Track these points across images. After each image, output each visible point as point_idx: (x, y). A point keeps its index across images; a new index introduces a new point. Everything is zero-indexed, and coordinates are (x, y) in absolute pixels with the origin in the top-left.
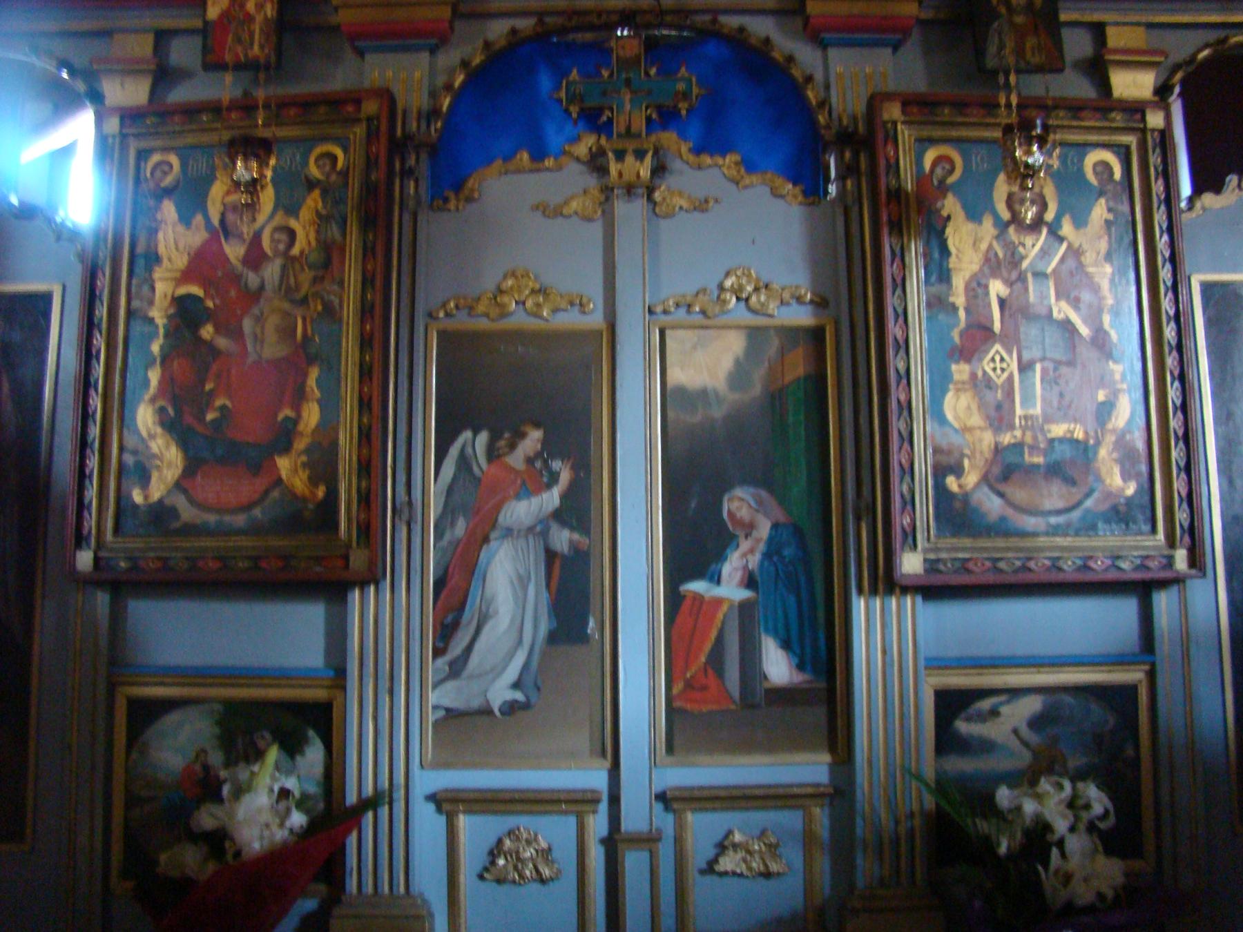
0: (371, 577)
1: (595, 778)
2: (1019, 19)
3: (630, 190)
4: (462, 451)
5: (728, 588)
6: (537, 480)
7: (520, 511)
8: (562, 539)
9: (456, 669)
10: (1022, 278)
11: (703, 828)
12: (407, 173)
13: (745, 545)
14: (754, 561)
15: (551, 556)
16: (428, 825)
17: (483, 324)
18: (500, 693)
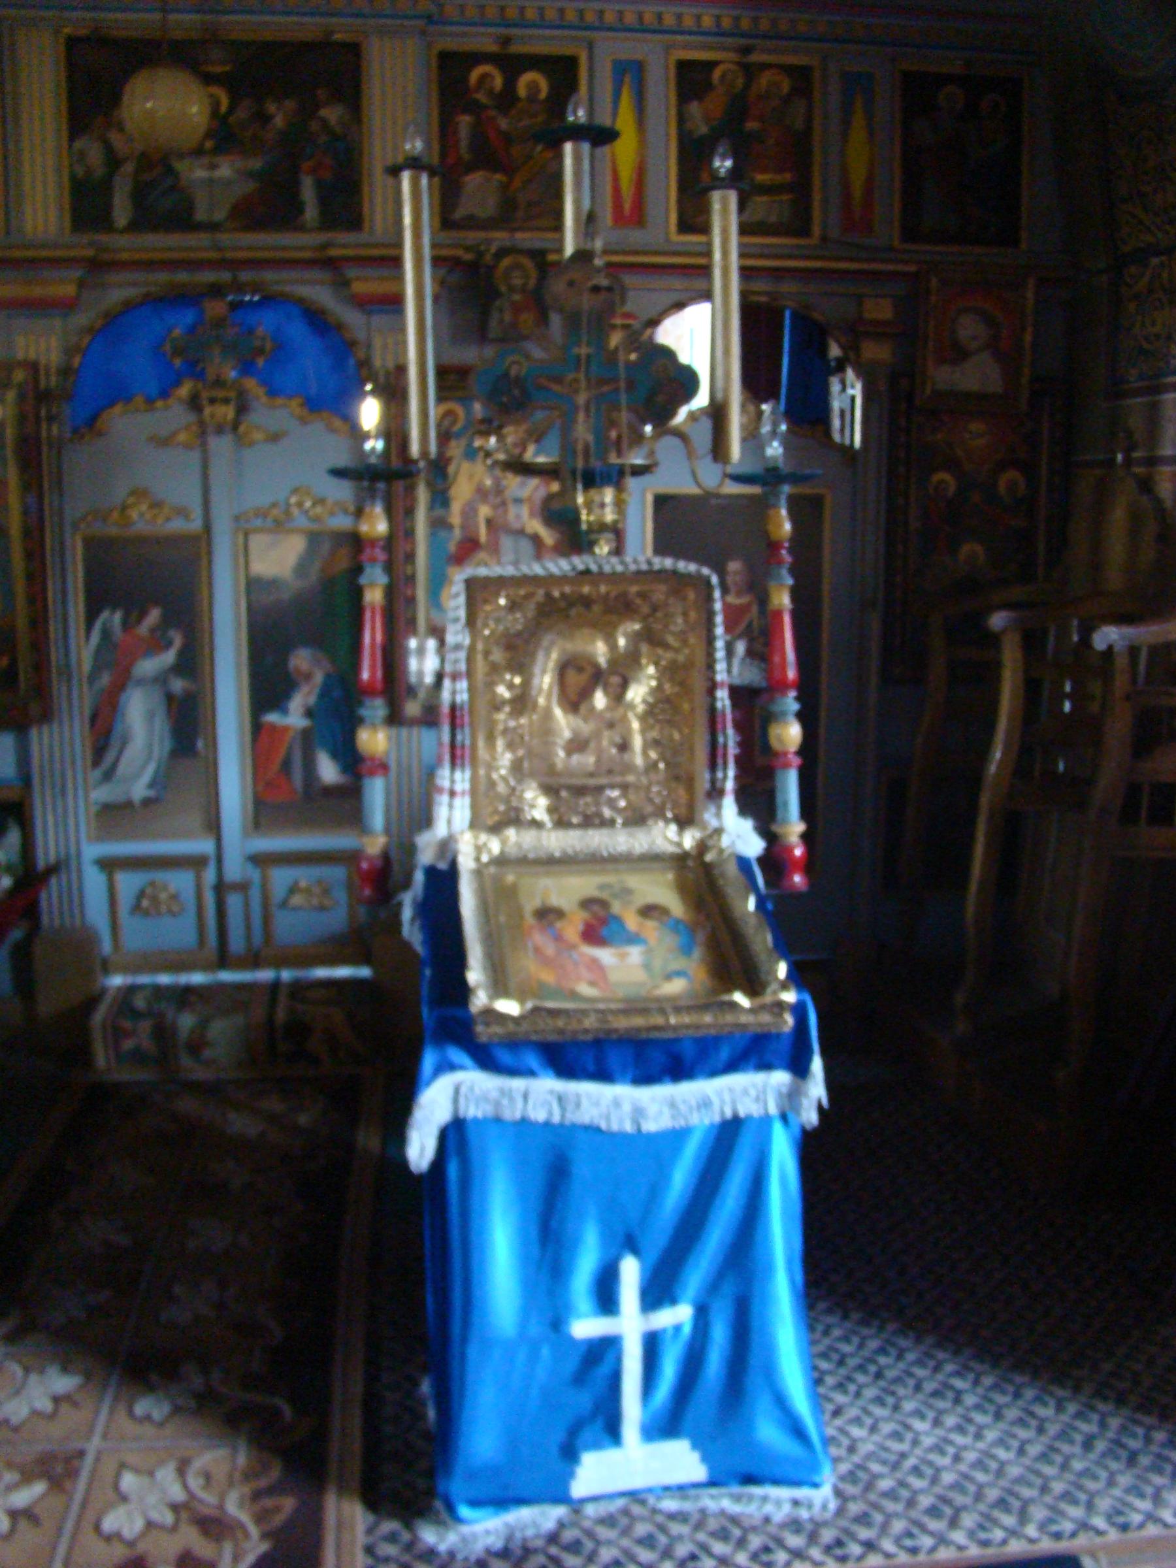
0: (46, 716)
1: (206, 846)
2: (517, 297)
3: (220, 430)
4: (104, 624)
5: (293, 717)
6: (158, 644)
7: (148, 666)
8: (178, 685)
9: (108, 776)
10: (504, 504)
11: (281, 877)
12: (51, 419)
13: (305, 689)
14: (312, 700)
15: (170, 698)
16: (94, 882)
17: (113, 531)
18: (139, 790)
